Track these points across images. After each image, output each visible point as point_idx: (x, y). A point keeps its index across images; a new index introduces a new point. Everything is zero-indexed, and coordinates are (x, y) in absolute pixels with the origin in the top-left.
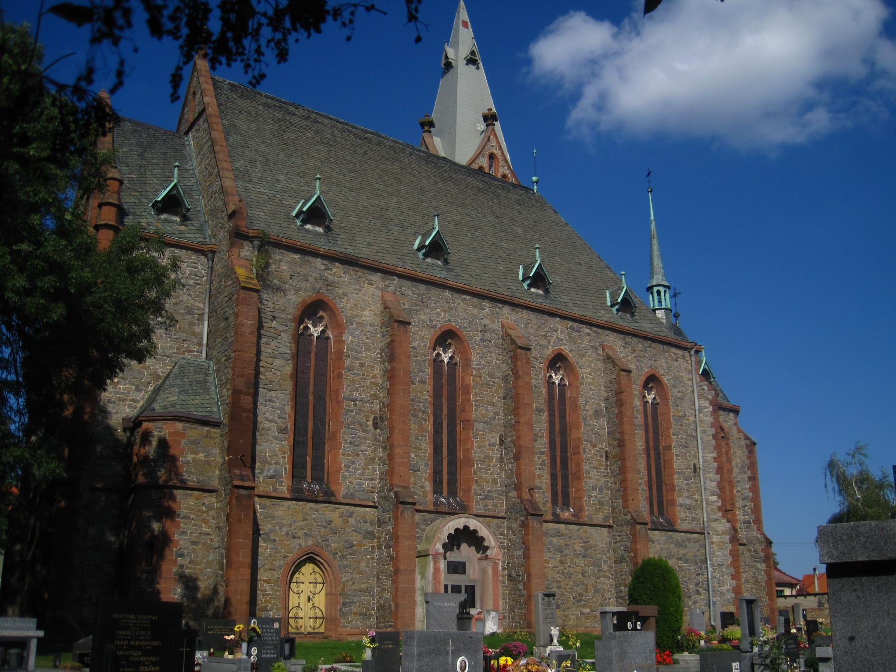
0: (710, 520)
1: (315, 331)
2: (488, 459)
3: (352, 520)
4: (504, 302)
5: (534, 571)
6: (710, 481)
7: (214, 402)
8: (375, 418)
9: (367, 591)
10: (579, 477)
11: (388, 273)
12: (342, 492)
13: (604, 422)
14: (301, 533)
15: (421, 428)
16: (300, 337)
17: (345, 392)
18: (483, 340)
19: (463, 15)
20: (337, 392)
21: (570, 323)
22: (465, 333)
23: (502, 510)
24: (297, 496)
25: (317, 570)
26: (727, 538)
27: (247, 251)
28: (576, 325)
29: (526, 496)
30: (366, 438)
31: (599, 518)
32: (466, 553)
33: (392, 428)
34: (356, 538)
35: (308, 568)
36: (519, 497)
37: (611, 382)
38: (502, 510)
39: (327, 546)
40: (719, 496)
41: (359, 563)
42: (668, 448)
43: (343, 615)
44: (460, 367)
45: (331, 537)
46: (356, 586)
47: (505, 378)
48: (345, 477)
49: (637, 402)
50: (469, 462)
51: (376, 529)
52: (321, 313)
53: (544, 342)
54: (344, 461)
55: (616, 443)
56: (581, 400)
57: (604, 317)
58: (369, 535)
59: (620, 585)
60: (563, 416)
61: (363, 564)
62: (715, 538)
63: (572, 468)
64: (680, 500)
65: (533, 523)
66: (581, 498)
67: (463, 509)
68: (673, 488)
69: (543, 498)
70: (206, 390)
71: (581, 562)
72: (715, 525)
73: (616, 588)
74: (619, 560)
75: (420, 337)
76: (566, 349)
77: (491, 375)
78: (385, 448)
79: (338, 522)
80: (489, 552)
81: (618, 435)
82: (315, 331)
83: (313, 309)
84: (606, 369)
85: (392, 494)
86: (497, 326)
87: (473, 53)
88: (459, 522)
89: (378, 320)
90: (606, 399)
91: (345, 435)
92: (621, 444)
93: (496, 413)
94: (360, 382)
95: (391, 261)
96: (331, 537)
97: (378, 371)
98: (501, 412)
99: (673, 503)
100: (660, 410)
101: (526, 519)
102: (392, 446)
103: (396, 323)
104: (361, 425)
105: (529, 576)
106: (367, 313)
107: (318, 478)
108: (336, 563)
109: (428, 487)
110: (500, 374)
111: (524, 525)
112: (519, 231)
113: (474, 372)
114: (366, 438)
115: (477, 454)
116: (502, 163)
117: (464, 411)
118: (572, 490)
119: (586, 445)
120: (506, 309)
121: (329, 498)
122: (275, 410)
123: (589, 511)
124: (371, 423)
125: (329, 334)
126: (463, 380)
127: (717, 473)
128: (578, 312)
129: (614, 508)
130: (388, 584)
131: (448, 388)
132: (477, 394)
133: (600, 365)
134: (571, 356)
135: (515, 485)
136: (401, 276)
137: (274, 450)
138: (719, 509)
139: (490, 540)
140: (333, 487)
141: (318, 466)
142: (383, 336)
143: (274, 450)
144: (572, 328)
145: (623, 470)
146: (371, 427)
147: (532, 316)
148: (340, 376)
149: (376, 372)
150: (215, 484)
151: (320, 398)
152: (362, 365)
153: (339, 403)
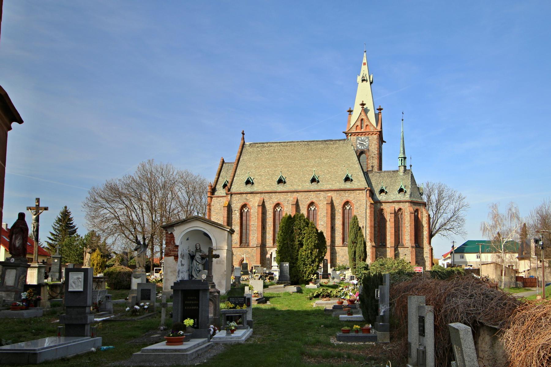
12: (251, 245)
15: (270, 228)
19: (365, 61)
24: (241, 246)
49: (341, 211)
76: (314, 200)
87: (363, 77)
91: (251, 233)
109: (272, 241)
120: (295, 193)
121: (248, 246)
147: (303, 193)
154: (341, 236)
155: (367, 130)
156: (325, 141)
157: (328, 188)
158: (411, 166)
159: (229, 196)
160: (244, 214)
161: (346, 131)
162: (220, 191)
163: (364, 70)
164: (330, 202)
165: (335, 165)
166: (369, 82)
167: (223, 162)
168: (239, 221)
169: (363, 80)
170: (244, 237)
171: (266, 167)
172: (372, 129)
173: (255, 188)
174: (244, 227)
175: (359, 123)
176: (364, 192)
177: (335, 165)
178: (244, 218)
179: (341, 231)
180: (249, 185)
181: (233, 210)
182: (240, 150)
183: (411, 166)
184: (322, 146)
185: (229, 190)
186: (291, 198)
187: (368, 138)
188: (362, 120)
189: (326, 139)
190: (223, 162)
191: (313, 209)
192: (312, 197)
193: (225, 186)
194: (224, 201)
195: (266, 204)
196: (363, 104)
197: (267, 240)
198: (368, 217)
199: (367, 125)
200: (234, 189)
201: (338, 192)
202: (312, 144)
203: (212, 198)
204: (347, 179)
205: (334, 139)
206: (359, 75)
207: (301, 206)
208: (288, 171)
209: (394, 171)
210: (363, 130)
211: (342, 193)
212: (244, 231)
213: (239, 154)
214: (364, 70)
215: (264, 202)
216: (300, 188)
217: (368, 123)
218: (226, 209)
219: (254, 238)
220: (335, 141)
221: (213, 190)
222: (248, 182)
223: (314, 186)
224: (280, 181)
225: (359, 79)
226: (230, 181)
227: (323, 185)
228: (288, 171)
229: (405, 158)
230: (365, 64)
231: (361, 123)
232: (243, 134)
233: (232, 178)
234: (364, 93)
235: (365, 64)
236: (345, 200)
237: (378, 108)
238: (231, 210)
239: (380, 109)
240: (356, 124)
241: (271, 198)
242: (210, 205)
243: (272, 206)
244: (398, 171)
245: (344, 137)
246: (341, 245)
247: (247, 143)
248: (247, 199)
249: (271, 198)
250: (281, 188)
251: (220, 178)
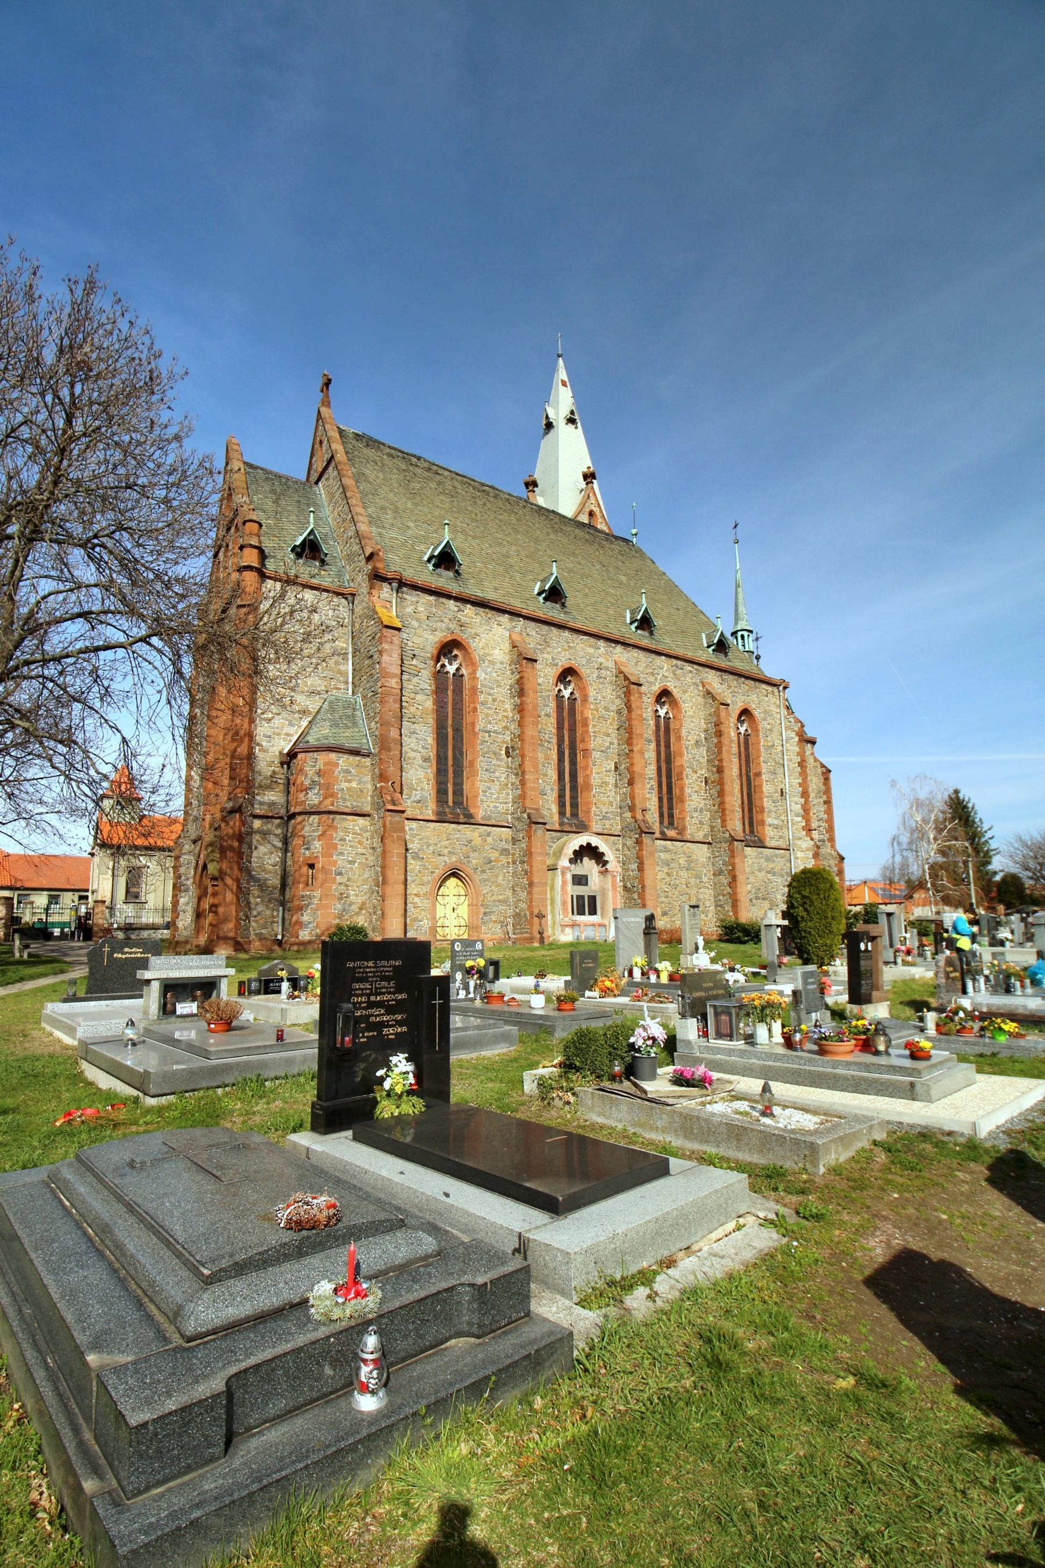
0: (794, 838)
1: (451, 669)
3: (489, 839)
4: (617, 642)
5: (647, 883)
6: (795, 804)
8: (507, 748)
9: (504, 902)
10: (682, 801)
11: (514, 614)
12: (480, 815)
13: (703, 751)
14: (446, 851)
16: (440, 675)
17: (480, 725)
18: (599, 677)
19: (562, 374)
20: (473, 724)
21: (675, 662)
22: (583, 671)
23: (617, 829)
24: (441, 819)
25: (460, 883)
26: (810, 854)
27: (386, 591)
28: (679, 663)
29: (639, 817)
30: (499, 766)
31: (700, 836)
32: (588, 866)
33: (523, 756)
34: (494, 855)
35: (453, 881)
36: (633, 817)
37: (710, 715)
38: (617, 829)
39: (469, 862)
40: (803, 817)
41: (497, 876)
42: (759, 774)
43: (484, 923)
44: (578, 702)
45: (472, 855)
46: (495, 898)
47: (619, 712)
48: (482, 801)
49: (733, 734)
50: (588, 787)
51: (510, 847)
52: (455, 652)
53: (652, 679)
54: (481, 786)
55: (715, 769)
56: (684, 732)
58: (505, 852)
59: (719, 894)
60: (668, 746)
61: (500, 878)
62: (799, 854)
63: (676, 791)
64: (769, 820)
65: (646, 839)
66: (684, 819)
67: (582, 828)
68: (762, 810)
69: (653, 817)
70: (355, 724)
71: (684, 874)
72: (799, 842)
73: (715, 897)
74: (718, 873)
75: (545, 675)
76: (671, 686)
77: (606, 709)
78: (517, 774)
79: (477, 841)
80: (608, 866)
81: (717, 763)
82: (451, 669)
83: (448, 648)
84: (706, 703)
85: (525, 816)
86: (611, 664)
87: (572, 413)
88: (582, 840)
89: (507, 659)
90: (706, 731)
91: (481, 763)
92: (720, 770)
93: (611, 743)
94: (492, 715)
95: (516, 604)
96: (472, 855)
97: (508, 706)
98: (615, 741)
99: (762, 823)
100: (751, 740)
101: (641, 836)
102: (523, 773)
103: (524, 660)
104: (495, 754)
105: (643, 887)
106: (497, 652)
107: (458, 803)
108: (477, 877)
110: (614, 708)
111: (639, 842)
112: (624, 579)
113: (592, 707)
114: (499, 766)
115: (595, 780)
116: (600, 520)
117: (583, 741)
118: (676, 812)
119: (688, 771)
120: (619, 649)
121: (469, 820)
122: (419, 741)
123: (690, 832)
124: (503, 752)
125: (463, 671)
126: (582, 712)
127: (802, 797)
128: (681, 652)
129: (712, 828)
130: (523, 895)
131: (569, 720)
132: (594, 726)
133: (701, 700)
134: (675, 692)
135: (629, 807)
136: (525, 618)
137: (419, 779)
138: (804, 828)
139: (609, 856)
140: (472, 810)
141: (458, 791)
142: (513, 673)
144: (676, 666)
145: (721, 794)
146: (504, 756)
147: (641, 655)
148: (475, 710)
149: (507, 706)
150: (367, 809)
151: (458, 730)
152: (494, 700)
153: (475, 734)
201: (726, 676)
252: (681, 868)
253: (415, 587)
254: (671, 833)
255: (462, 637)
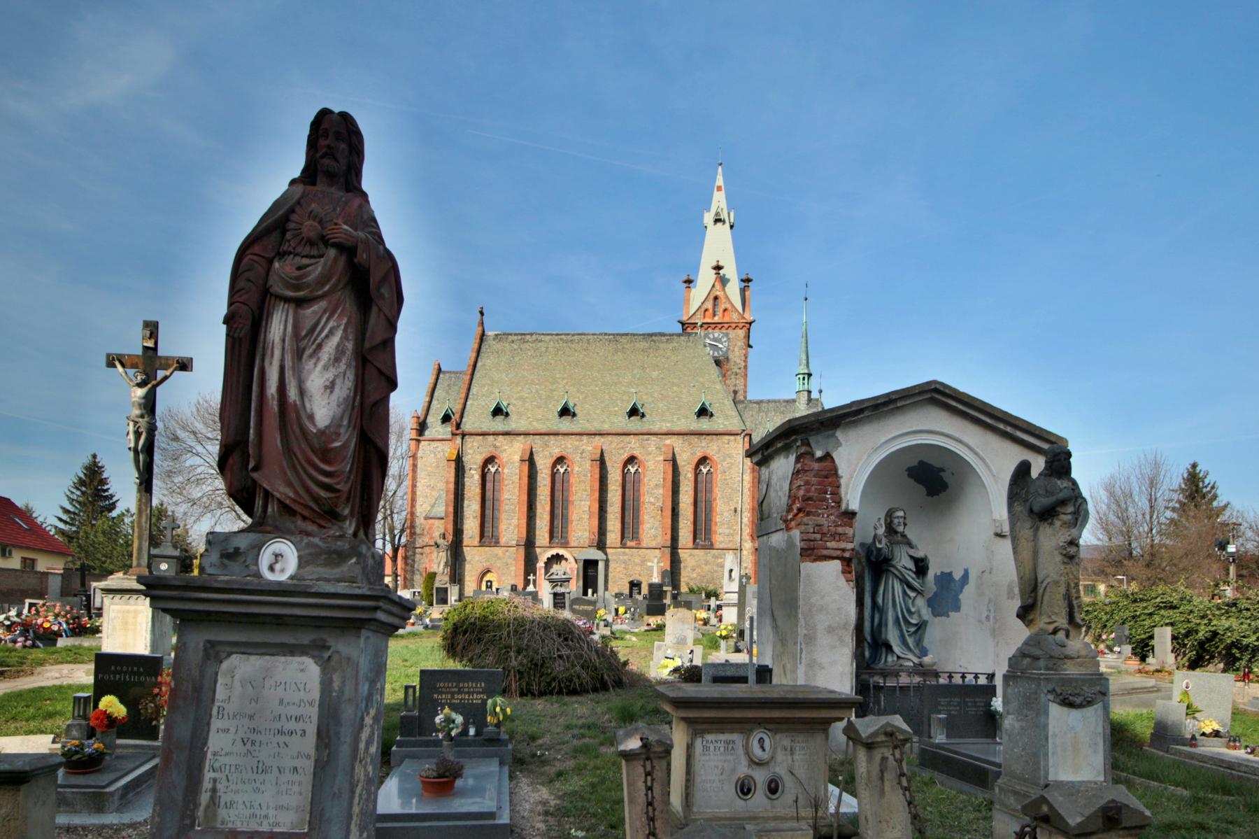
2: (581, 519)
7: (440, 510)
12: (503, 541)
13: (661, 491)
19: (720, 181)
22: (570, 457)
31: (653, 544)
34: (510, 561)
49: (691, 476)
57: (682, 425)
67: (565, 545)
71: (638, 568)
76: (636, 453)
83: (490, 460)
87: (717, 214)
88: (554, 552)
109: (547, 536)
112: (655, 374)
120: (597, 438)
121: (497, 543)
143: (471, 525)
147: (615, 438)
154: (691, 528)
155: (726, 319)
156: (651, 335)
157: (664, 429)
158: (821, 392)
159: (459, 440)
160: (489, 478)
161: (684, 319)
162: (436, 428)
163: (719, 201)
164: (670, 456)
165: (674, 384)
166: (727, 225)
167: (439, 370)
168: (478, 490)
169: (717, 221)
170: (488, 525)
171: (533, 383)
172: (735, 317)
173: (513, 424)
174: (489, 504)
175: (709, 305)
176: (739, 438)
177: (674, 384)
178: (489, 486)
179: (691, 517)
180: (500, 418)
181: (467, 469)
182: (476, 346)
183: (821, 392)
184: (644, 344)
185: (458, 426)
186: (590, 447)
187: (727, 335)
188: (716, 298)
189: (651, 331)
190: (439, 370)
191: (633, 470)
192: (633, 446)
193: (446, 419)
194: (449, 450)
195: (536, 458)
196: (718, 268)
197: (537, 533)
198: (746, 490)
199: (725, 310)
200: (467, 426)
202: (624, 340)
203: (418, 441)
204: (703, 412)
205: (667, 331)
206: (709, 210)
207: (609, 464)
208: (578, 391)
209: (787, 401)
210: (716, 319)
211: (695, 439)
212: (489, 512)
213: (474, 355)
214: (719, 201)
215: (531, 453)
216: (606, 427)
217: (728, 306)
218: (453, 465)
219: (511, 526)
220: (670, 335)
221: (422, 427)
222: (498, 411)
223: (635, 424)
224: (565, 412)
225: (708, 218)
226: (457, 408)
227: (654, 422)
228: (578, 391)
229: (810, 375)
230: (719, 189)
231: (714, 305)
232: (482, 313)
233: (462, 401)
234: (718, 245)
235: (719, 189)
236: (699, 455)
237: (744, 277)
238: (463, 467)
239: (749, 280)
240: (705, 306)
241: (547, 446)
242: (414, 457)
243: (550, 462)
244: (794, 401)
245: (679, 329)
246: (690, 545)
247: (490, 333)
248: (495, 447)
249: (547, 446)
250: (566, 425)
251: (434, 402)
252: (636, 564)
253: (471, 434)
254: (633, 544)
255: (496, 453)
